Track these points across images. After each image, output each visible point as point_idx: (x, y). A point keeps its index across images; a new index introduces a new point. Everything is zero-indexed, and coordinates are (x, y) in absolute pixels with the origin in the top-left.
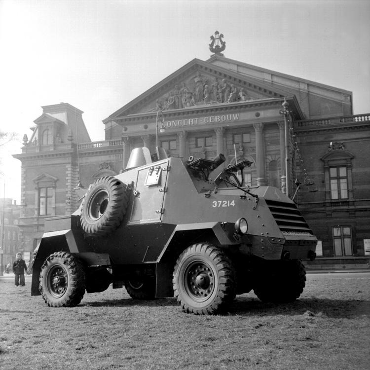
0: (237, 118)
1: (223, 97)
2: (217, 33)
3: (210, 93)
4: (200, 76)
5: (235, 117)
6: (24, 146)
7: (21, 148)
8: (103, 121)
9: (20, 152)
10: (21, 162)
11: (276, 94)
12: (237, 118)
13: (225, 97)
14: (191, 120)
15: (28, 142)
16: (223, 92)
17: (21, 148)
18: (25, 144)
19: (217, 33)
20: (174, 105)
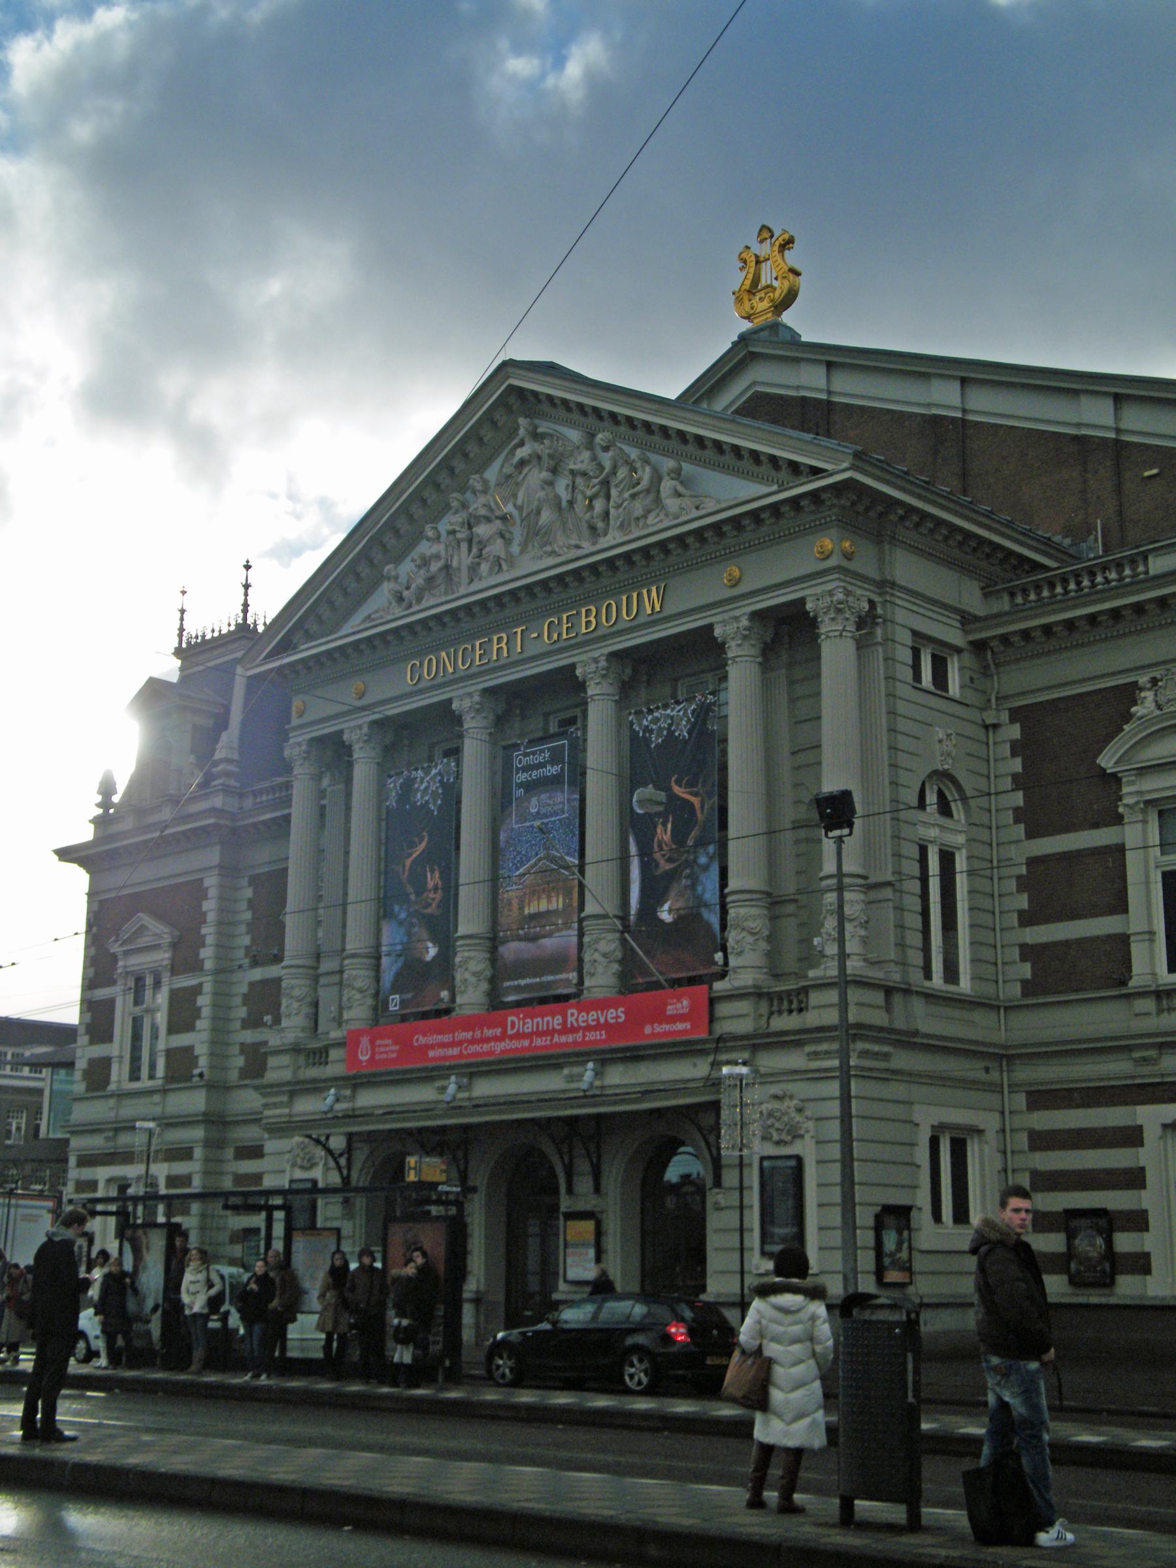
0: (657, 608)
1: (606, 514)
2: (766, 231)
4: (536, 436)
5: (651, 600)
6: (100, 811)
7: (90, 821)
9: (85, 834)
10: (88, 876)
11: (794, 467)
12: (657, 608)
13: (612, 511)
14: (500, 640)
15: (116, 799)
17: (90, 821)
18: (105, 804)
19: (766, 231)
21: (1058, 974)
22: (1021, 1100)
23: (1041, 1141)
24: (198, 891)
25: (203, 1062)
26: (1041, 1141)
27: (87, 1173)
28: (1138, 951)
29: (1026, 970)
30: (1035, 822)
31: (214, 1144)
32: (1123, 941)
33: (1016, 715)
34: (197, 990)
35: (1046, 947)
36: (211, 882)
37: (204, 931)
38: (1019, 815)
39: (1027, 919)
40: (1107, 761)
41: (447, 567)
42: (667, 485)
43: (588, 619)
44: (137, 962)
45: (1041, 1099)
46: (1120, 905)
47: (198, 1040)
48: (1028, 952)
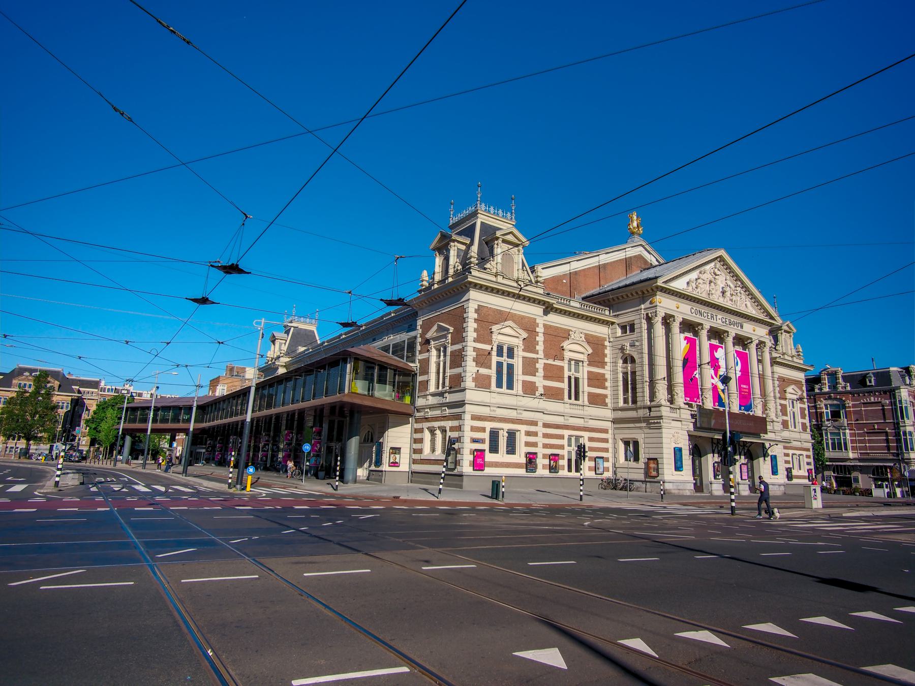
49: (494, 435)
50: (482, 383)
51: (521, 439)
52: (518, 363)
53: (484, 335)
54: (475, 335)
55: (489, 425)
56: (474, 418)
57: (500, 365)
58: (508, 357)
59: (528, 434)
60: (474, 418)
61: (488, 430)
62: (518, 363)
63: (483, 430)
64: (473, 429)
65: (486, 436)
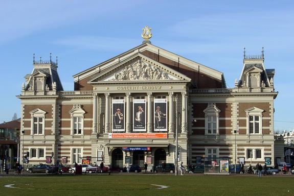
1: (153, 76)
3: (146, 73)
4: (140, 62)
8: (73, 76)
11: (181, 78)
16: (153, 73)
20: (125, 78)
21: (196, 132)
22: (191, 145)
23: (193, 149)
24: (51, 106)
25: (54, 132)
26: (193, 149)
27: (25, 147)
28: (206, 131)
29: (192, 132)
30: (195, 116)
31: (56, 144)
32: (204, 130)
33: (193, 104)
34: (52, 121)
35: (195, 130)
36: (54, 105)
37: (52, 112)
38: (192, 115)
39: (193, 126)
40: (204, 111)
41: (125, 76)
42: (162, 75)
43: (148, 87)
44: (35, 115)
45: (194, 145)
46: (204, 126)
47: (53, 129)
48: (193, 130)
49: (249, 151)
50: (242, 132)
51: (263, 152)
52: (260, 122)
53: (241, 113)
54: (238, 114)
55: (246, 148)
56: (238, 145)
57: (251, 125)
58: (255, 120)
59: (265, 150)
60: (238, 145)
61: (246, 150)
62: (260, 122)
63: (243, 150)
64: (238, 150)
65: (245, 152)
